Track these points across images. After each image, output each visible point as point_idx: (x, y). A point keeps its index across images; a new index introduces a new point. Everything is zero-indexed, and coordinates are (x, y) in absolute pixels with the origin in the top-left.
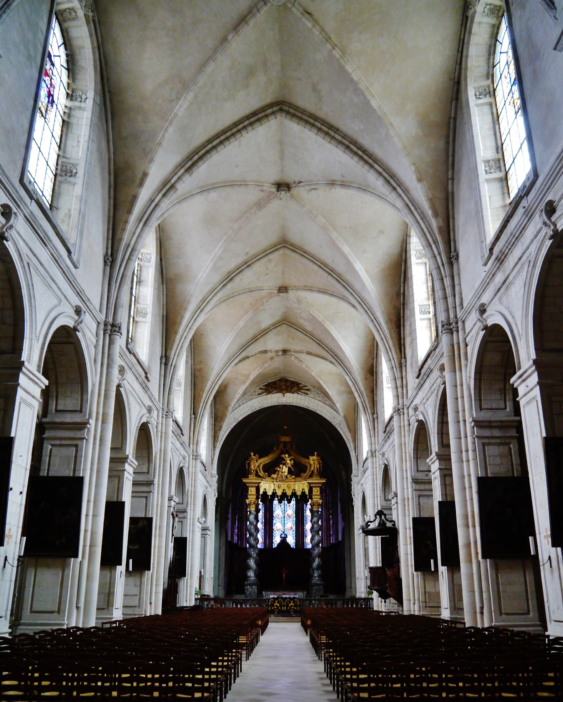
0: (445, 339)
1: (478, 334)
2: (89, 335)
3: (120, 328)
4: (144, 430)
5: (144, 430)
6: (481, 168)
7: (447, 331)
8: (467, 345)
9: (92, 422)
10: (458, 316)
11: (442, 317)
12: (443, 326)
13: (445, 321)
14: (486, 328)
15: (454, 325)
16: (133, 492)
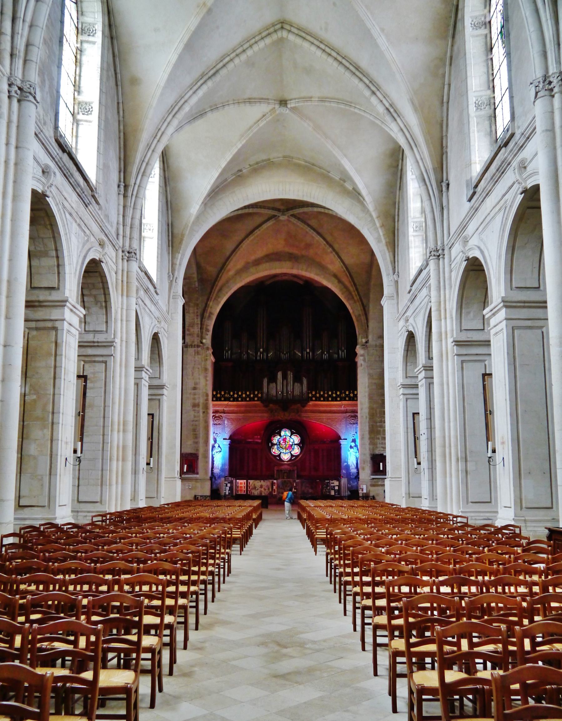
0: (432, 264)
1: (460, 265)
2: (110, 262)
3: (135, 254)
4: (156, 338)
5: (156, 338)
6: (472, 109)
7: (434, 257)
8: (451, 271)
9: (118, 340)
10: (446, 243)
11: (431, 245)
12: (431, 252)
13: (433, 247)
14: (468, 259)
15: (440, 252)
16: (149, 395)
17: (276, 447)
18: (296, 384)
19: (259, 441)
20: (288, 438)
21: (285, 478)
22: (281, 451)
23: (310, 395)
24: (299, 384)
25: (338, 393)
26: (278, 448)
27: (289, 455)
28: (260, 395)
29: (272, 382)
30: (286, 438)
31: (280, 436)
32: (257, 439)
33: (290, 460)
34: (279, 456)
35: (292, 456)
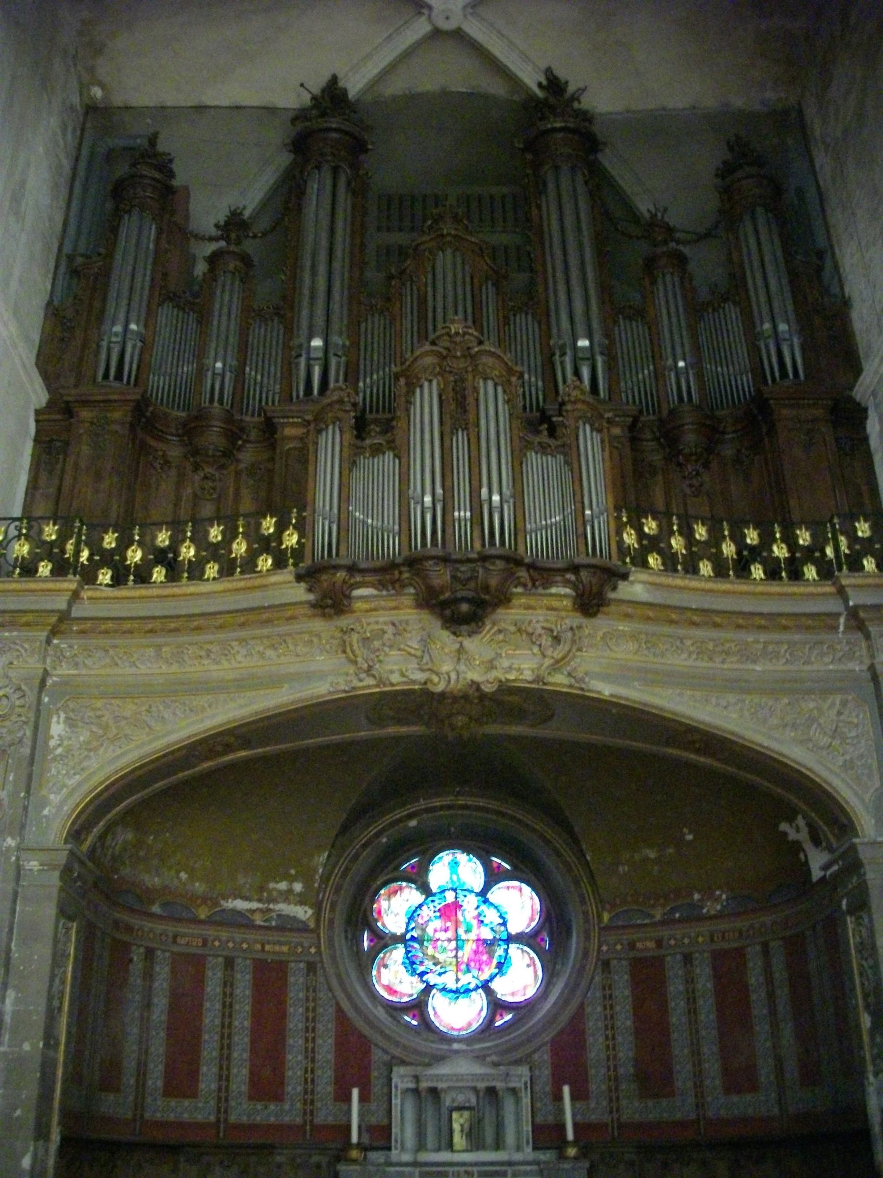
17: (398, 953)
18: (534, 459)
19: (303, 913)
20: (470, 903)
21: (459, 1140)
22: (432, 979)
23: (630, 538)
24: (553, 463)
25: (804, 538)
26: (411, 963)
27: (479, 1000)
28: (291, 539)
29: (377, 451)
30: (456, 906)
31: (425, 889)
32: (287, 896)
33: (488, 1025)
34: (419, 1006)
35: (497, 1005)
